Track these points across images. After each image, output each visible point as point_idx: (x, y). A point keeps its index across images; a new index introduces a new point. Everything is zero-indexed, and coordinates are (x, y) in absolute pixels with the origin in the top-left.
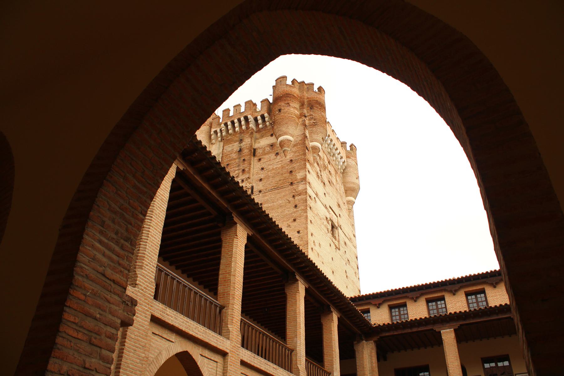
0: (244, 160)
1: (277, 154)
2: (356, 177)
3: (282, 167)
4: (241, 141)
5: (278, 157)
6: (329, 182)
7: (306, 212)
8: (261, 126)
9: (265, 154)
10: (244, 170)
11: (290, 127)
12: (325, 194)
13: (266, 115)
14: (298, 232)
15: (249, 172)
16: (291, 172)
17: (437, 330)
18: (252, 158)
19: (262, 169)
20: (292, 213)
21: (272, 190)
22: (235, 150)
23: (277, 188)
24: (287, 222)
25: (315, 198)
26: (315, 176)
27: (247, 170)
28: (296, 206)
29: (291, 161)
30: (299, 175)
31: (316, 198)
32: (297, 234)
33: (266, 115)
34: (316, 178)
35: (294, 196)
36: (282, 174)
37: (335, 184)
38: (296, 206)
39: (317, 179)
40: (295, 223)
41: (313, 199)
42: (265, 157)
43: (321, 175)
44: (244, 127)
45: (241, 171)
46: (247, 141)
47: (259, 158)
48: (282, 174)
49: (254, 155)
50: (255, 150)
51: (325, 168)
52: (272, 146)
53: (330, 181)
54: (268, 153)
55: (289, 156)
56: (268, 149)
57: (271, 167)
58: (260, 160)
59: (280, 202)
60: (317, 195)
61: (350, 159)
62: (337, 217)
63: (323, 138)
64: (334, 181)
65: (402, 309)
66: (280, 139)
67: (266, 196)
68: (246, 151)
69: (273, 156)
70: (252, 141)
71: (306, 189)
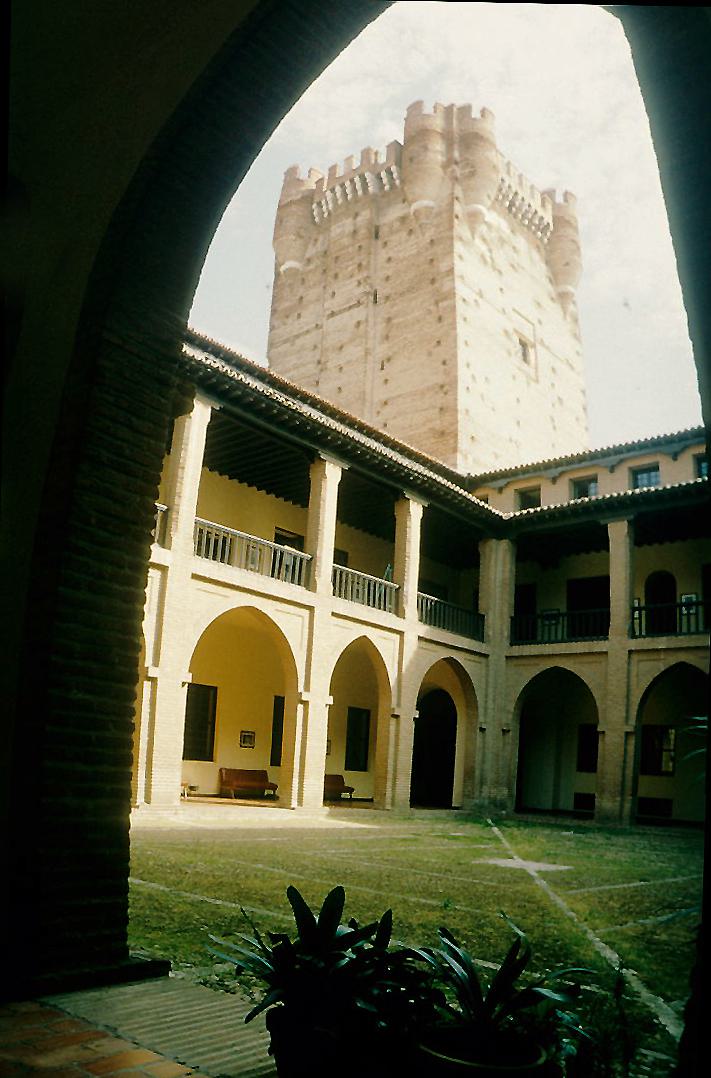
1: (411, 232)
3: (419, 254)
4: (357, 215)
5: (413, 237)
6: (513, 266)
9: (392, 232)
10: (360, 265)
12: (501, 290)
13: (393, 168)
14: (444, 363)
15: (367, 268)
16: (432, 260)
18: (373, 242)
19: (389, 259)
21: (402, 294)
22: (347, 232)
23: (410, 290)
25: (476, 301)
27: (364, 263)
28: (440, 319)
29: (432, 241)
31: (480, 301)
32: (442, 367)
33: (393, 168)
35: (437, 303)
36: (418, 266)
38: (440, 319)
40: (439, 348)
41: (472, 302)
43: (492, 258)
44: (360, 193)
45: (356, 266)
46: (365, 215)
48: (418, 266)
49: (377, 237)
52: (403, 219)
54: (398, 231)
55: (429, 234)
56: (397, 225)
57: (401, 255)
59: (417, 314)
62: (533, 325)
65: (653, 474)
66: (414, 206)
67: (395, 305)
68: (363, 232)
69: (404, 234)
70: (371, 213)
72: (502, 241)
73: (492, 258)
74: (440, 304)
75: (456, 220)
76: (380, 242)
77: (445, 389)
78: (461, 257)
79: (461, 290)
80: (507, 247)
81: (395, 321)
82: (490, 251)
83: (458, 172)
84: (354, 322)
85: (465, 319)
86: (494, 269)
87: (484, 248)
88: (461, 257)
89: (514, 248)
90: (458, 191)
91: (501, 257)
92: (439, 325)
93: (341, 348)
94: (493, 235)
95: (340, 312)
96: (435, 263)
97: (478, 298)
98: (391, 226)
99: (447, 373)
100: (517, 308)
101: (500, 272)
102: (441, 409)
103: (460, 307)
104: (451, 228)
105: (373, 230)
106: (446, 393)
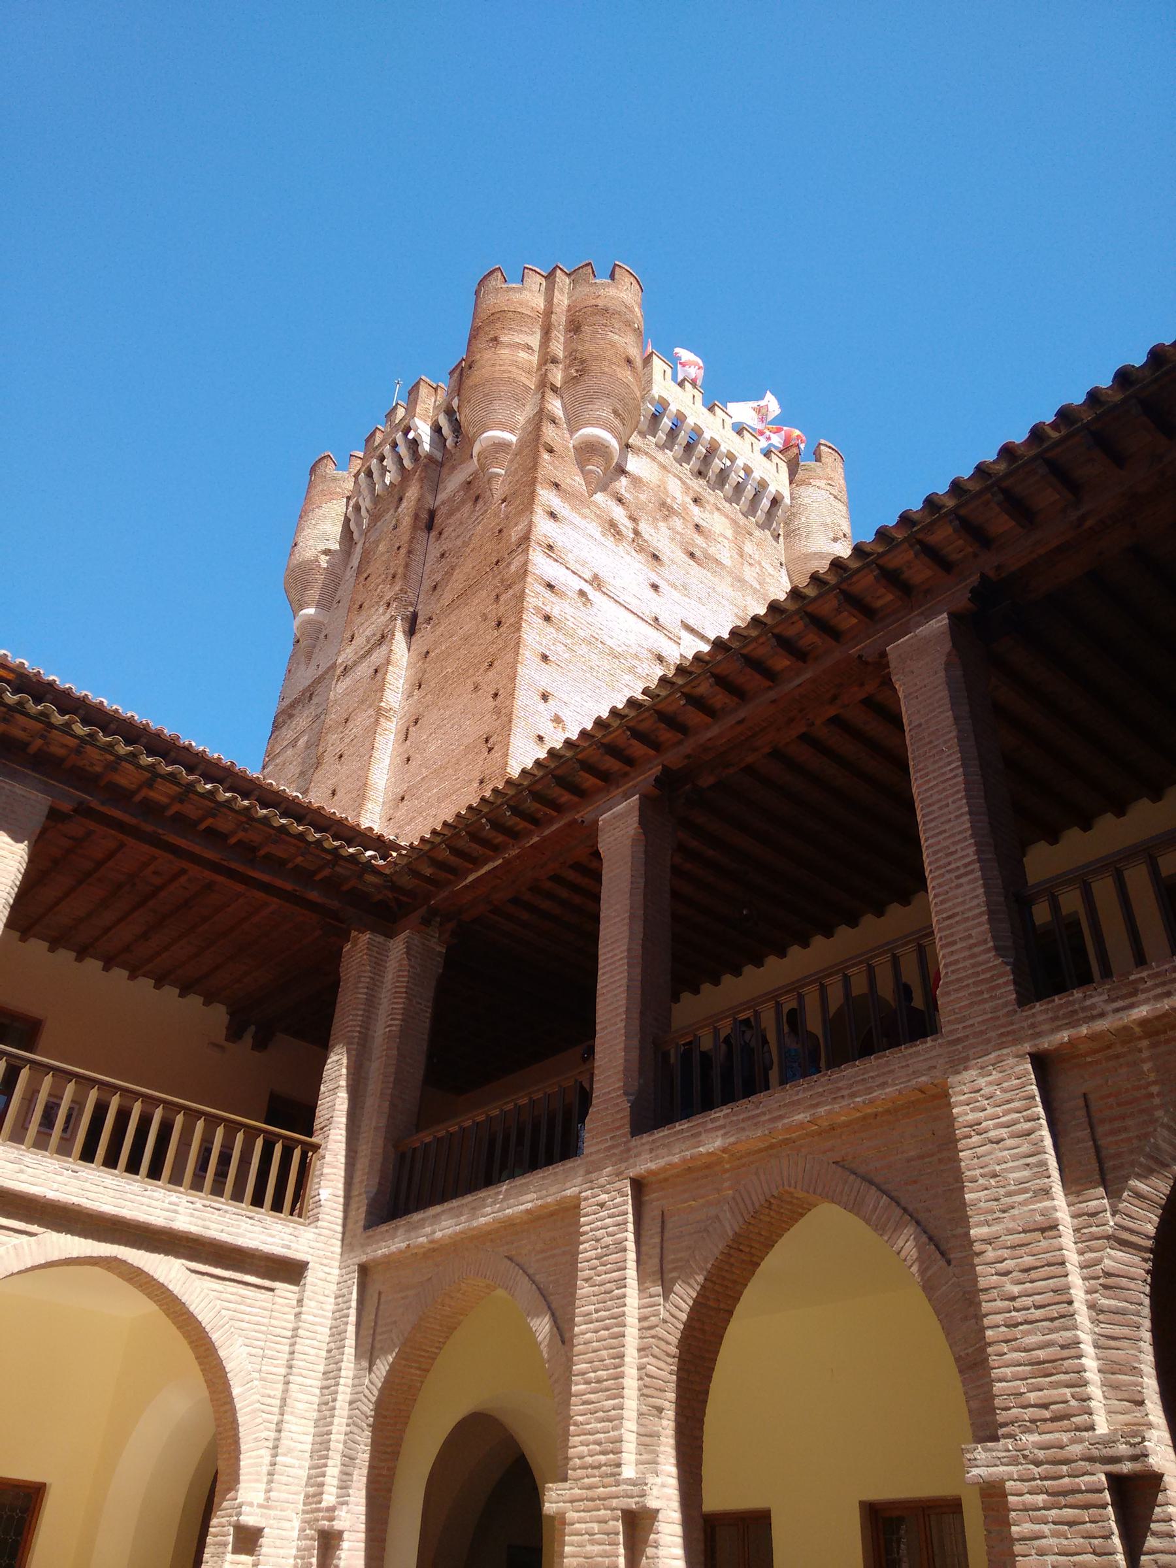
0: (399, 548)
2: (832, 535)
6: (692, 555)
7: (519, 629)
8: (449, 443)
9: (451, 514)
11: (497, 405)
12: (655, 587)
17: (589, 818)
18: (421, 535)
19: (442, 555)
20: (486, 649)
24: (474, 679)
25: (582, 593)
26: (594, 529)
30: (514, 535)
32: (491, 703)
34: (603, 539)
37: (727, 561)
39: (609, 542)
42: (451, 521)
43: (636, 533)
44: (407, 463)
47: (440, 529)
49: (429, 527)
50: (432, 514)
51: (666, 510)
53: (698, 554)
54: (463, 502)
58: (440, 534)
60: (596, 581)
61: (810, 488)
63: (616, 413)
64: (725, 554)
66: (476, 449)
71: (526, 563)
72: (666, 510)
73: (636, 533)
74: (503, 598)
75: (546, 456)
76: (433, 534)
77: (491, 741)
78: (552, 515)
79: (541, 564)
80: (677, 523)
81: (432, 654)
82: (633, 519)
83: (557, 376)
84: (372, 671)
85: (547, 618)
86: (640, 549)
87: (618, 513)
88: (552, 515)
89: (697, 526)
90: (555, 406)
91: (659, 536)
92: (496, 633)
93: (347, 721)
94: (643, 497)
95: (355, 664)
96: (504, 534)
97: (587, 588)
98: (451, 499)
99: (497, 711)
100: (691, 623)
101: (655, 557)
102: (481, 782)
103: (535, 596)
104: (535, 466)
105: (424, 516)
106: (490, 750)
